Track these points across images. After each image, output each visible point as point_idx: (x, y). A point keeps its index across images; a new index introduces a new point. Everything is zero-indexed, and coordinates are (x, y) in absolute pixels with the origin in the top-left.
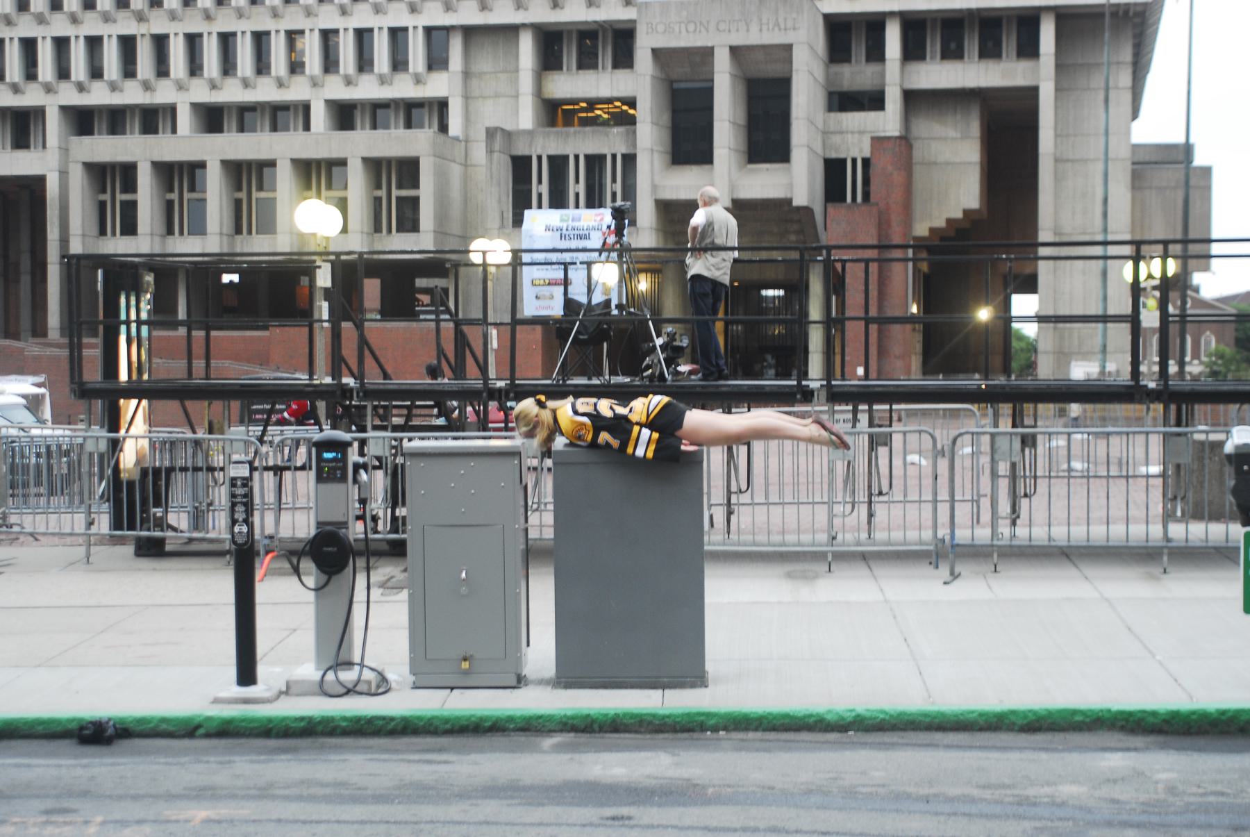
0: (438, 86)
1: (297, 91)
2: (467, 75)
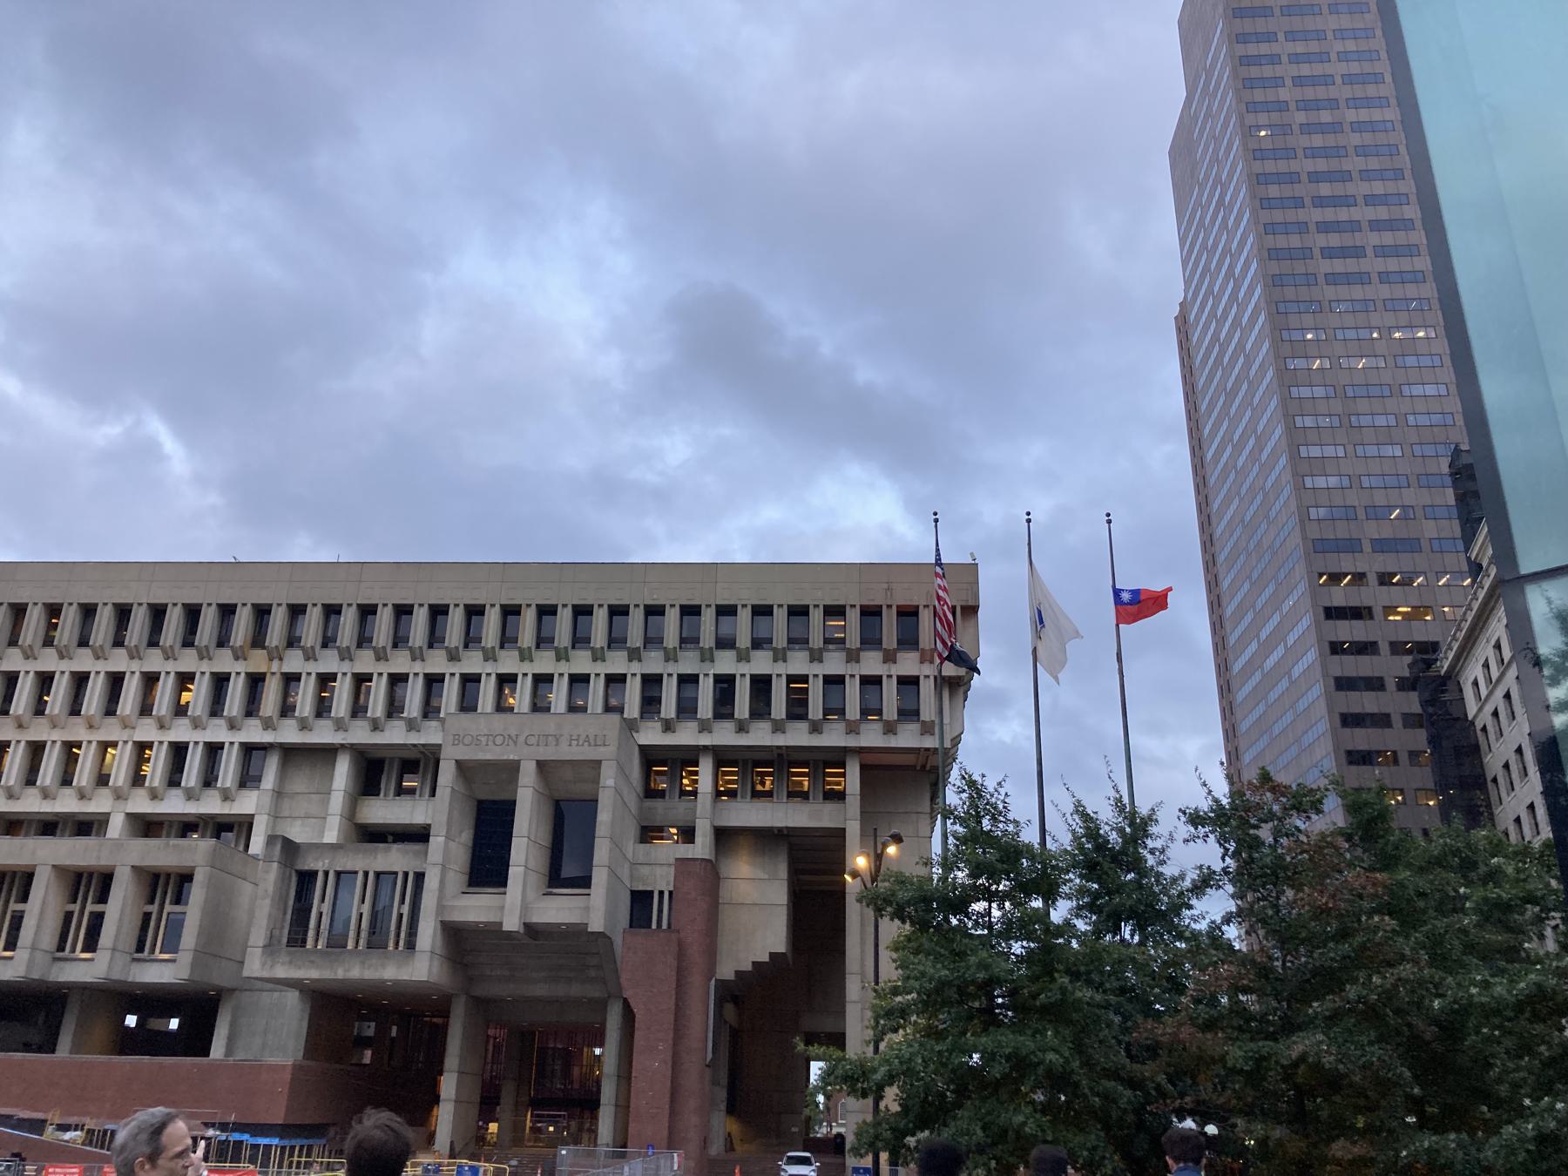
0: (247, 803)
1: (100, 804)
2: (279, 794)
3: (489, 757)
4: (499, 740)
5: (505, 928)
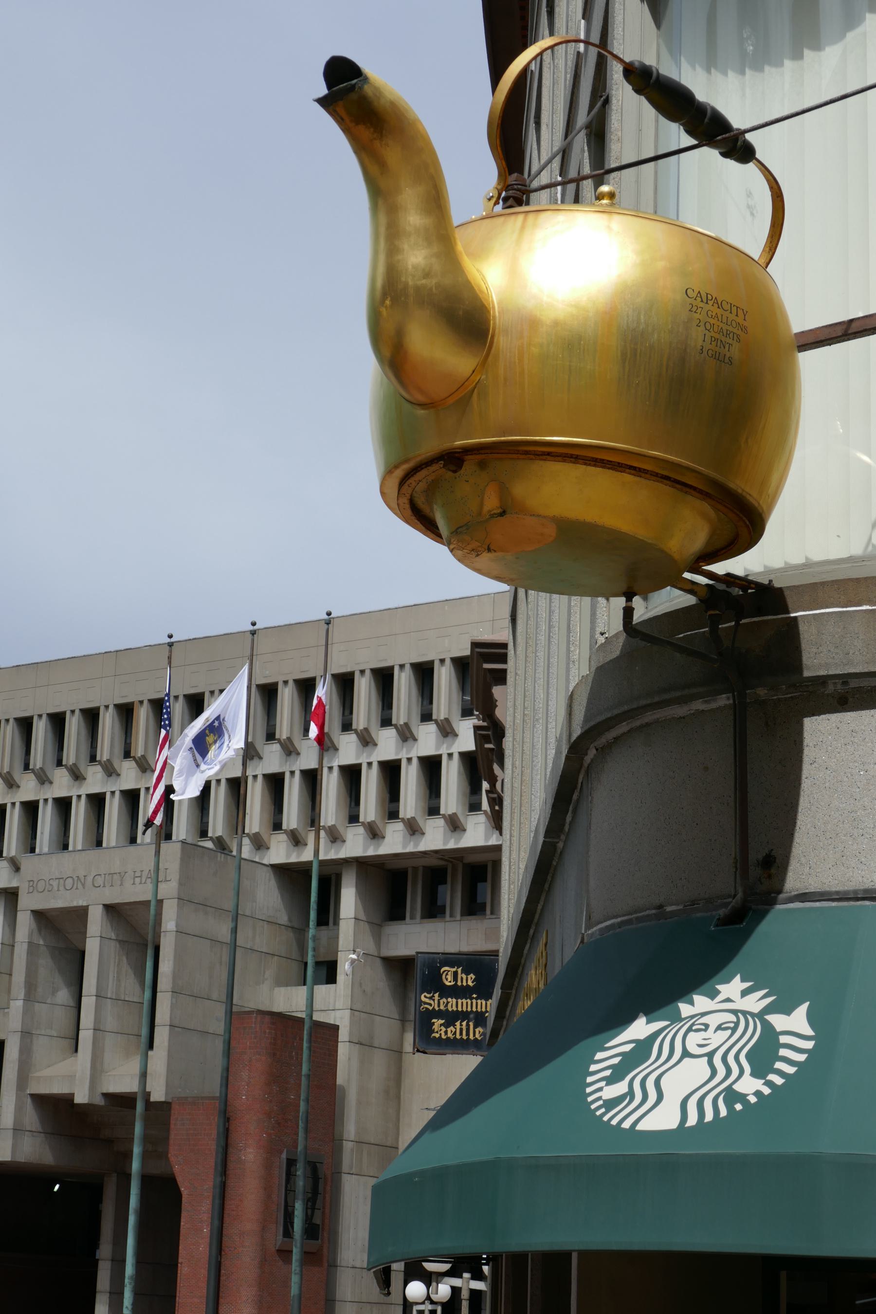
3: (59, 904)
4: (69, 882)
5: (78, 1100)
